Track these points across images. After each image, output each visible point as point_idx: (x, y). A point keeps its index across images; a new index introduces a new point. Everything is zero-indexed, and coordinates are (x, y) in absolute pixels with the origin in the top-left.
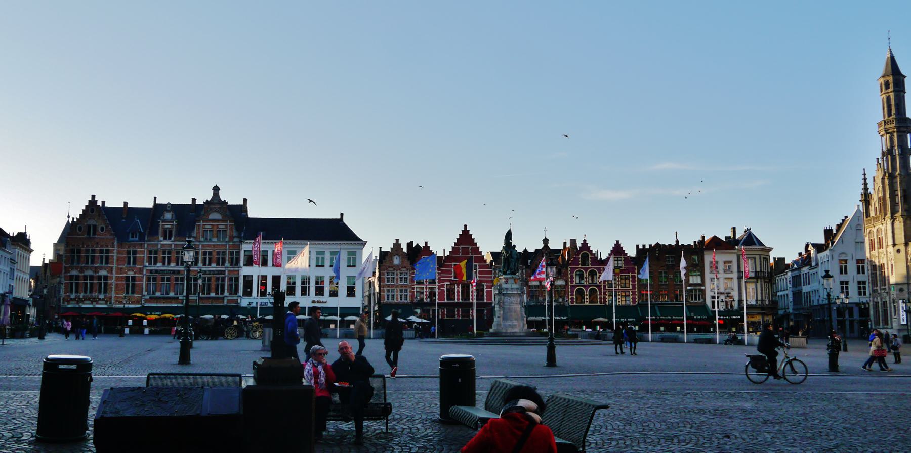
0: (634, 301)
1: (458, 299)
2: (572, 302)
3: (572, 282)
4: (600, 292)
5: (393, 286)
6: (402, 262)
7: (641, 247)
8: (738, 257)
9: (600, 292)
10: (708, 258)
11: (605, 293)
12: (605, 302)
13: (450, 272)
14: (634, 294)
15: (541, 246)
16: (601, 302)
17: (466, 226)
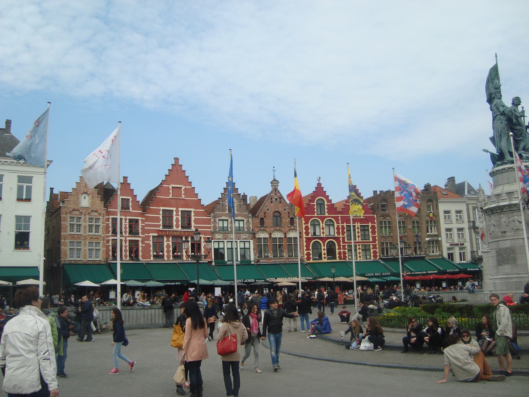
0: (375, 256)
1: (168, 257)
2: (309, 259)
3: (307, 233)
4: (339, 245)
5: (79, 237)
6: (93, 204)
7: (378, 193)
8: (468, 205)
9: (339, 245)
10: (442, 207)
11: (344, 248)
12: (345, 258)
13: (158, 219)
14: (374, 247)
15: (267, 190)
16: (340, 258)
17: (176, 159)
